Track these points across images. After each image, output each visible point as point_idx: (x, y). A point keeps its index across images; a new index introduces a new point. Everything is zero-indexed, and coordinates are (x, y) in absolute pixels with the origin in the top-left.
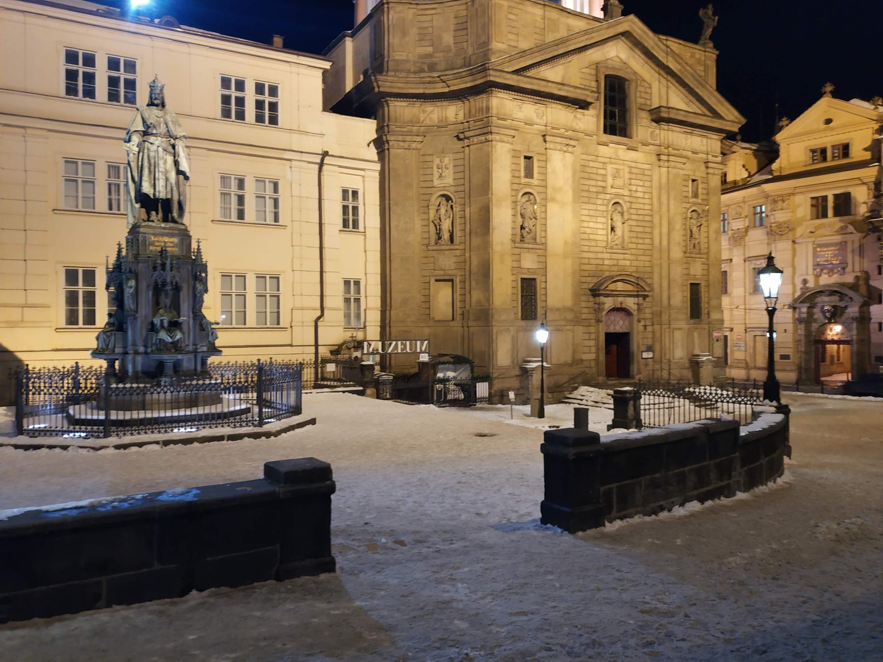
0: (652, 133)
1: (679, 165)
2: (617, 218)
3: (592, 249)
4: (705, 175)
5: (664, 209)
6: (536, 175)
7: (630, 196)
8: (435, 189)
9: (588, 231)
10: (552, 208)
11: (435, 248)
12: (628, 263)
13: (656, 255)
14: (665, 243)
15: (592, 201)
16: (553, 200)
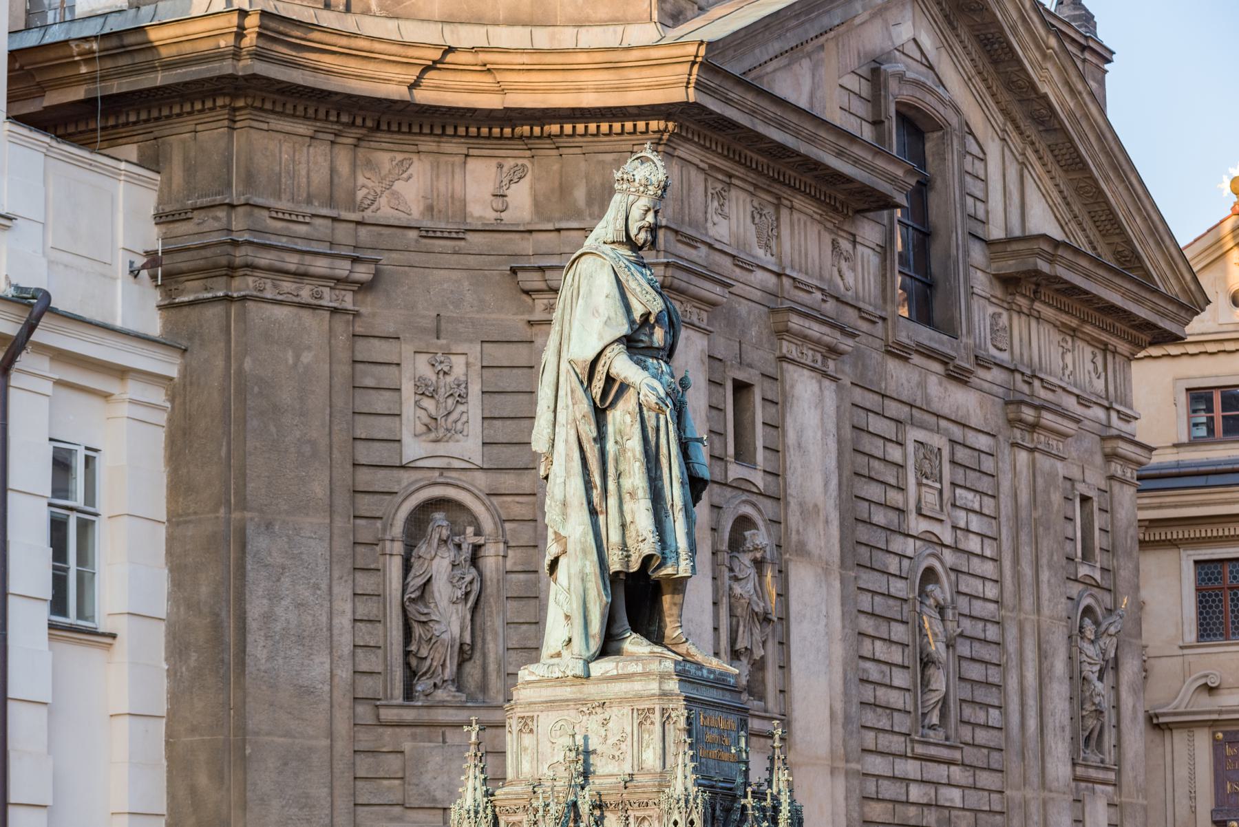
0: (995, 316)
1: (1055, 444)
2: (931, 623)
3: (885, 741)
4: (1103, 484)
5: (1028, 603)
6: (760, 455)
7: (956, 549)
8: (406, 477)
9: (873, 671)
10: (803, 580)
11: (409, 715)
12: (953, 796)
13: (1014, 767)
14: (1032, 723)
15: (880, 559)
16: (802, 551)
